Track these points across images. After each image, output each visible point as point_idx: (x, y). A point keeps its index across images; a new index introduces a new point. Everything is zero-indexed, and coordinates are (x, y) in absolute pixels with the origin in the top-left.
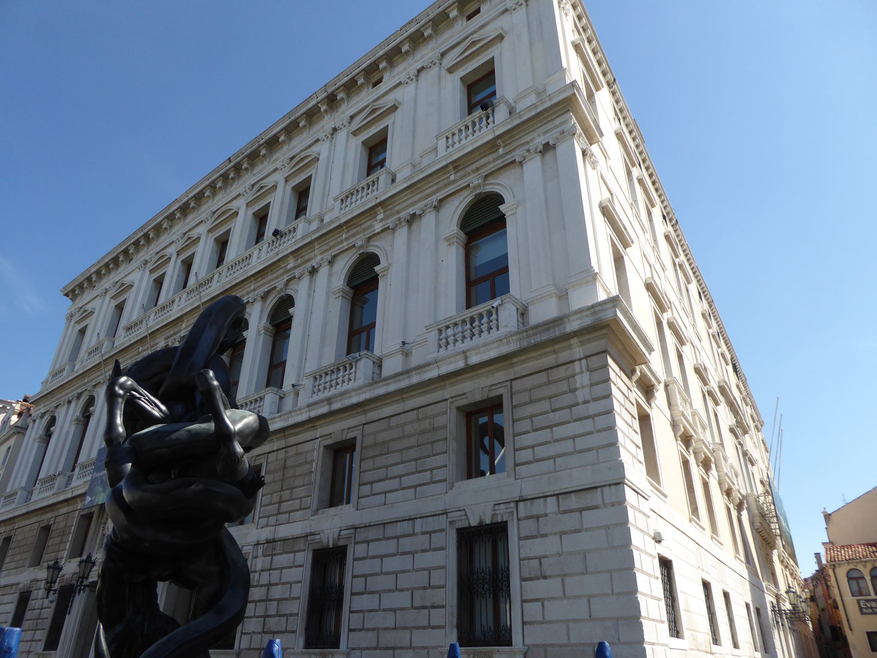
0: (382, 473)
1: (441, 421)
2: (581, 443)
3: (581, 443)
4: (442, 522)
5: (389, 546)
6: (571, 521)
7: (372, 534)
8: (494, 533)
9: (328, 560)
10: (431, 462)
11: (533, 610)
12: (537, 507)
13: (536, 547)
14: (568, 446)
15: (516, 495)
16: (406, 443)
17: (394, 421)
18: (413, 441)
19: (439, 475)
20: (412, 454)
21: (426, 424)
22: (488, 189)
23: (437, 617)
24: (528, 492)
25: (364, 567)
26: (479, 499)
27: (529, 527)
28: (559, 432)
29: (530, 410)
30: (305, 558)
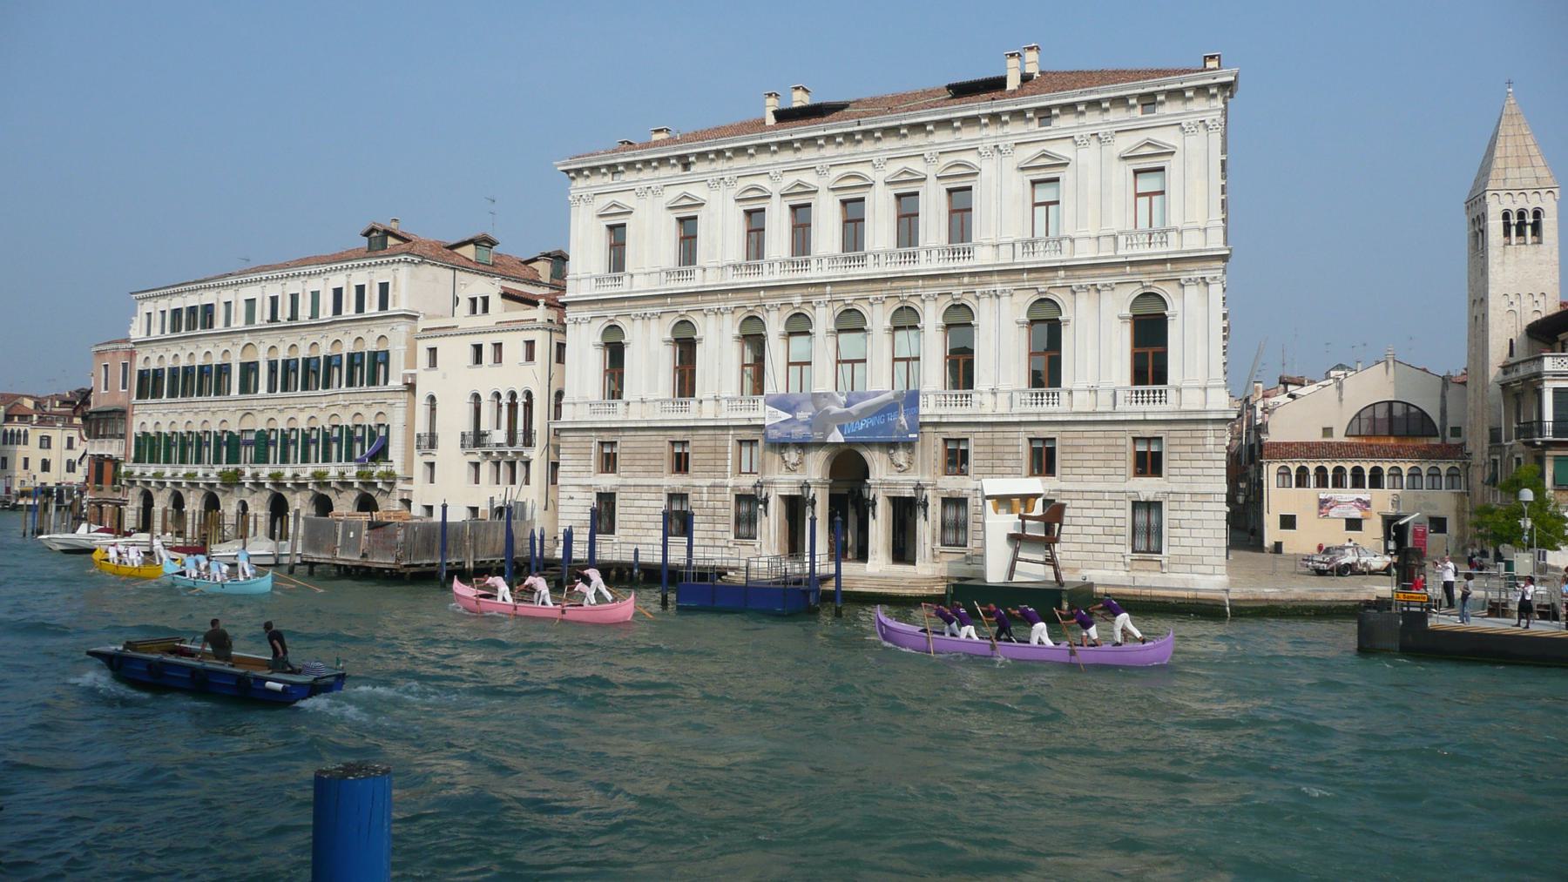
1: (1122, 442)
2: (1206, 472)
3: (1206, 472)
7: (1074, 496)
8: (1153, 506)
10: (1113, 464)
11: (1175, 541)
12: (1180, 498)
13: (1179, 515)
14: (1199, 472)
16: (1095, 449)
21: (1110, 442)
26: (1147, 487)
27: (1175, 505)
28: (1195, 464)
29: (1179, 449)
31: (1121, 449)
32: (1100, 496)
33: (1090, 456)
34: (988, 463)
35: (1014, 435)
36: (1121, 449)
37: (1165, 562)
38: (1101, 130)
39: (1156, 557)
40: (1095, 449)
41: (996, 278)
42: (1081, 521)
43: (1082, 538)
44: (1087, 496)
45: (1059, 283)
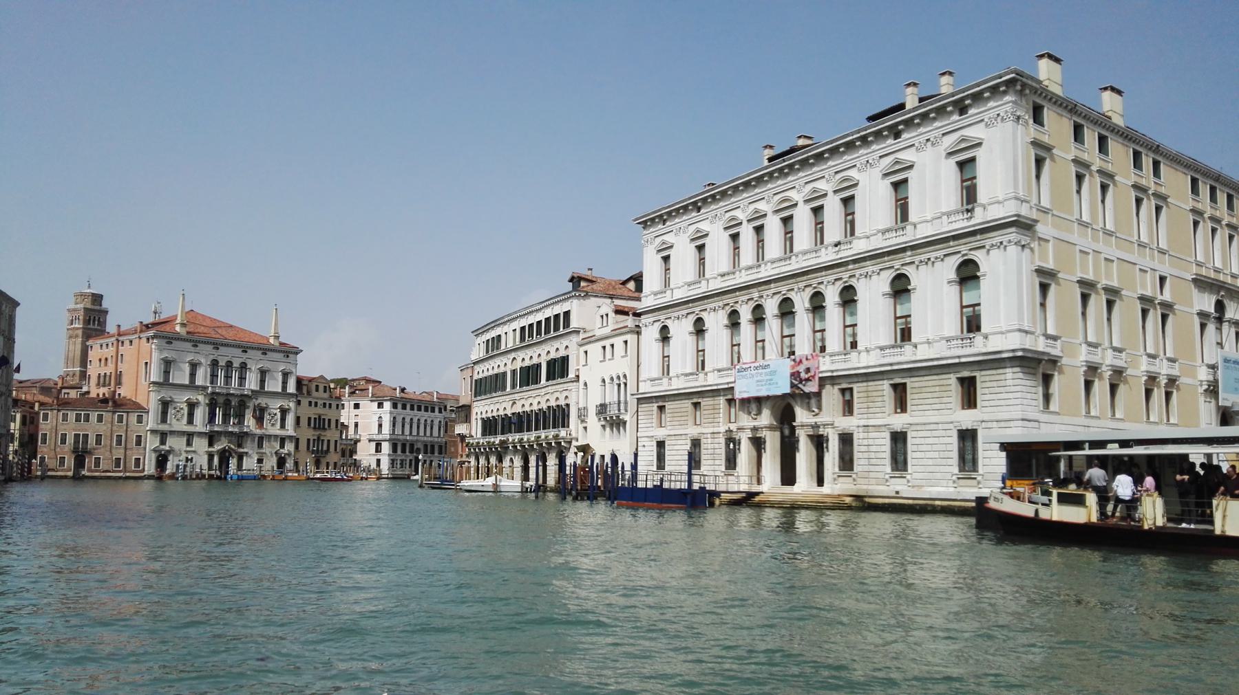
4: (951, 426)
7: (919, 428)
9: (899, 439)
12: (989, 425)
16: (932, 389)
19: (949, 406)
20: (935, 395)
22: (970, 257)
23: (950, 462)
30: (887, 436)
31: (948, 388)
33: (929, 395)
34: (865, 405)
37: (979, 478)
38: (931, 136)
39: (974, 475)
40: (932, 389)
41: (868, 263)
43: (925, 462)
44: (928, 427)
45: (908, 260)
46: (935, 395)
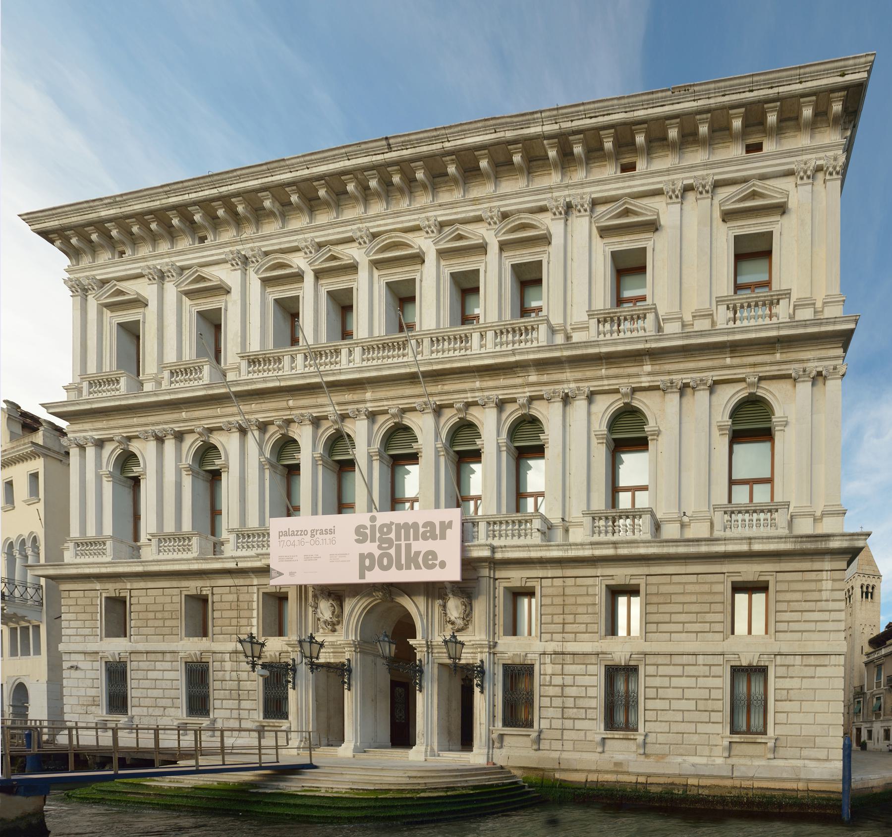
0: (666, 618)
5: (678, 670)
6: (809, 671)
7: (660, 660)
13: (787, 683)
15: (776, 650)
17: (675, 579)
18: (693, 598)
20: (695, 608)
21: (706, 588)
24: (784, 650)
25: (657, 682)
27: (782, 671)
32: (691, 659)
35: (590, 581)
36: (719, 598)
42: (670, 693)
43: (669, 716)
44: (677, 660)
46: (695, 608)
